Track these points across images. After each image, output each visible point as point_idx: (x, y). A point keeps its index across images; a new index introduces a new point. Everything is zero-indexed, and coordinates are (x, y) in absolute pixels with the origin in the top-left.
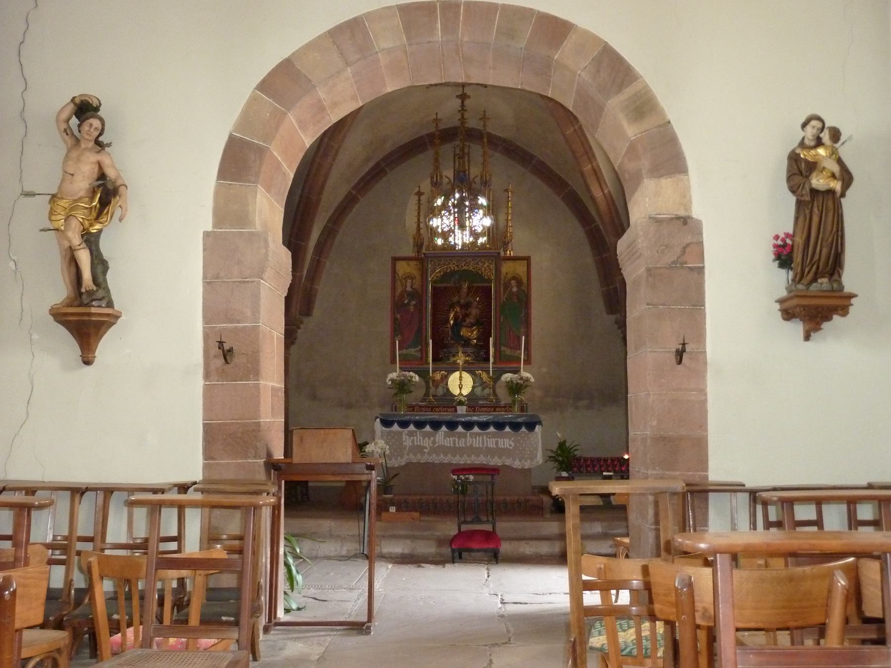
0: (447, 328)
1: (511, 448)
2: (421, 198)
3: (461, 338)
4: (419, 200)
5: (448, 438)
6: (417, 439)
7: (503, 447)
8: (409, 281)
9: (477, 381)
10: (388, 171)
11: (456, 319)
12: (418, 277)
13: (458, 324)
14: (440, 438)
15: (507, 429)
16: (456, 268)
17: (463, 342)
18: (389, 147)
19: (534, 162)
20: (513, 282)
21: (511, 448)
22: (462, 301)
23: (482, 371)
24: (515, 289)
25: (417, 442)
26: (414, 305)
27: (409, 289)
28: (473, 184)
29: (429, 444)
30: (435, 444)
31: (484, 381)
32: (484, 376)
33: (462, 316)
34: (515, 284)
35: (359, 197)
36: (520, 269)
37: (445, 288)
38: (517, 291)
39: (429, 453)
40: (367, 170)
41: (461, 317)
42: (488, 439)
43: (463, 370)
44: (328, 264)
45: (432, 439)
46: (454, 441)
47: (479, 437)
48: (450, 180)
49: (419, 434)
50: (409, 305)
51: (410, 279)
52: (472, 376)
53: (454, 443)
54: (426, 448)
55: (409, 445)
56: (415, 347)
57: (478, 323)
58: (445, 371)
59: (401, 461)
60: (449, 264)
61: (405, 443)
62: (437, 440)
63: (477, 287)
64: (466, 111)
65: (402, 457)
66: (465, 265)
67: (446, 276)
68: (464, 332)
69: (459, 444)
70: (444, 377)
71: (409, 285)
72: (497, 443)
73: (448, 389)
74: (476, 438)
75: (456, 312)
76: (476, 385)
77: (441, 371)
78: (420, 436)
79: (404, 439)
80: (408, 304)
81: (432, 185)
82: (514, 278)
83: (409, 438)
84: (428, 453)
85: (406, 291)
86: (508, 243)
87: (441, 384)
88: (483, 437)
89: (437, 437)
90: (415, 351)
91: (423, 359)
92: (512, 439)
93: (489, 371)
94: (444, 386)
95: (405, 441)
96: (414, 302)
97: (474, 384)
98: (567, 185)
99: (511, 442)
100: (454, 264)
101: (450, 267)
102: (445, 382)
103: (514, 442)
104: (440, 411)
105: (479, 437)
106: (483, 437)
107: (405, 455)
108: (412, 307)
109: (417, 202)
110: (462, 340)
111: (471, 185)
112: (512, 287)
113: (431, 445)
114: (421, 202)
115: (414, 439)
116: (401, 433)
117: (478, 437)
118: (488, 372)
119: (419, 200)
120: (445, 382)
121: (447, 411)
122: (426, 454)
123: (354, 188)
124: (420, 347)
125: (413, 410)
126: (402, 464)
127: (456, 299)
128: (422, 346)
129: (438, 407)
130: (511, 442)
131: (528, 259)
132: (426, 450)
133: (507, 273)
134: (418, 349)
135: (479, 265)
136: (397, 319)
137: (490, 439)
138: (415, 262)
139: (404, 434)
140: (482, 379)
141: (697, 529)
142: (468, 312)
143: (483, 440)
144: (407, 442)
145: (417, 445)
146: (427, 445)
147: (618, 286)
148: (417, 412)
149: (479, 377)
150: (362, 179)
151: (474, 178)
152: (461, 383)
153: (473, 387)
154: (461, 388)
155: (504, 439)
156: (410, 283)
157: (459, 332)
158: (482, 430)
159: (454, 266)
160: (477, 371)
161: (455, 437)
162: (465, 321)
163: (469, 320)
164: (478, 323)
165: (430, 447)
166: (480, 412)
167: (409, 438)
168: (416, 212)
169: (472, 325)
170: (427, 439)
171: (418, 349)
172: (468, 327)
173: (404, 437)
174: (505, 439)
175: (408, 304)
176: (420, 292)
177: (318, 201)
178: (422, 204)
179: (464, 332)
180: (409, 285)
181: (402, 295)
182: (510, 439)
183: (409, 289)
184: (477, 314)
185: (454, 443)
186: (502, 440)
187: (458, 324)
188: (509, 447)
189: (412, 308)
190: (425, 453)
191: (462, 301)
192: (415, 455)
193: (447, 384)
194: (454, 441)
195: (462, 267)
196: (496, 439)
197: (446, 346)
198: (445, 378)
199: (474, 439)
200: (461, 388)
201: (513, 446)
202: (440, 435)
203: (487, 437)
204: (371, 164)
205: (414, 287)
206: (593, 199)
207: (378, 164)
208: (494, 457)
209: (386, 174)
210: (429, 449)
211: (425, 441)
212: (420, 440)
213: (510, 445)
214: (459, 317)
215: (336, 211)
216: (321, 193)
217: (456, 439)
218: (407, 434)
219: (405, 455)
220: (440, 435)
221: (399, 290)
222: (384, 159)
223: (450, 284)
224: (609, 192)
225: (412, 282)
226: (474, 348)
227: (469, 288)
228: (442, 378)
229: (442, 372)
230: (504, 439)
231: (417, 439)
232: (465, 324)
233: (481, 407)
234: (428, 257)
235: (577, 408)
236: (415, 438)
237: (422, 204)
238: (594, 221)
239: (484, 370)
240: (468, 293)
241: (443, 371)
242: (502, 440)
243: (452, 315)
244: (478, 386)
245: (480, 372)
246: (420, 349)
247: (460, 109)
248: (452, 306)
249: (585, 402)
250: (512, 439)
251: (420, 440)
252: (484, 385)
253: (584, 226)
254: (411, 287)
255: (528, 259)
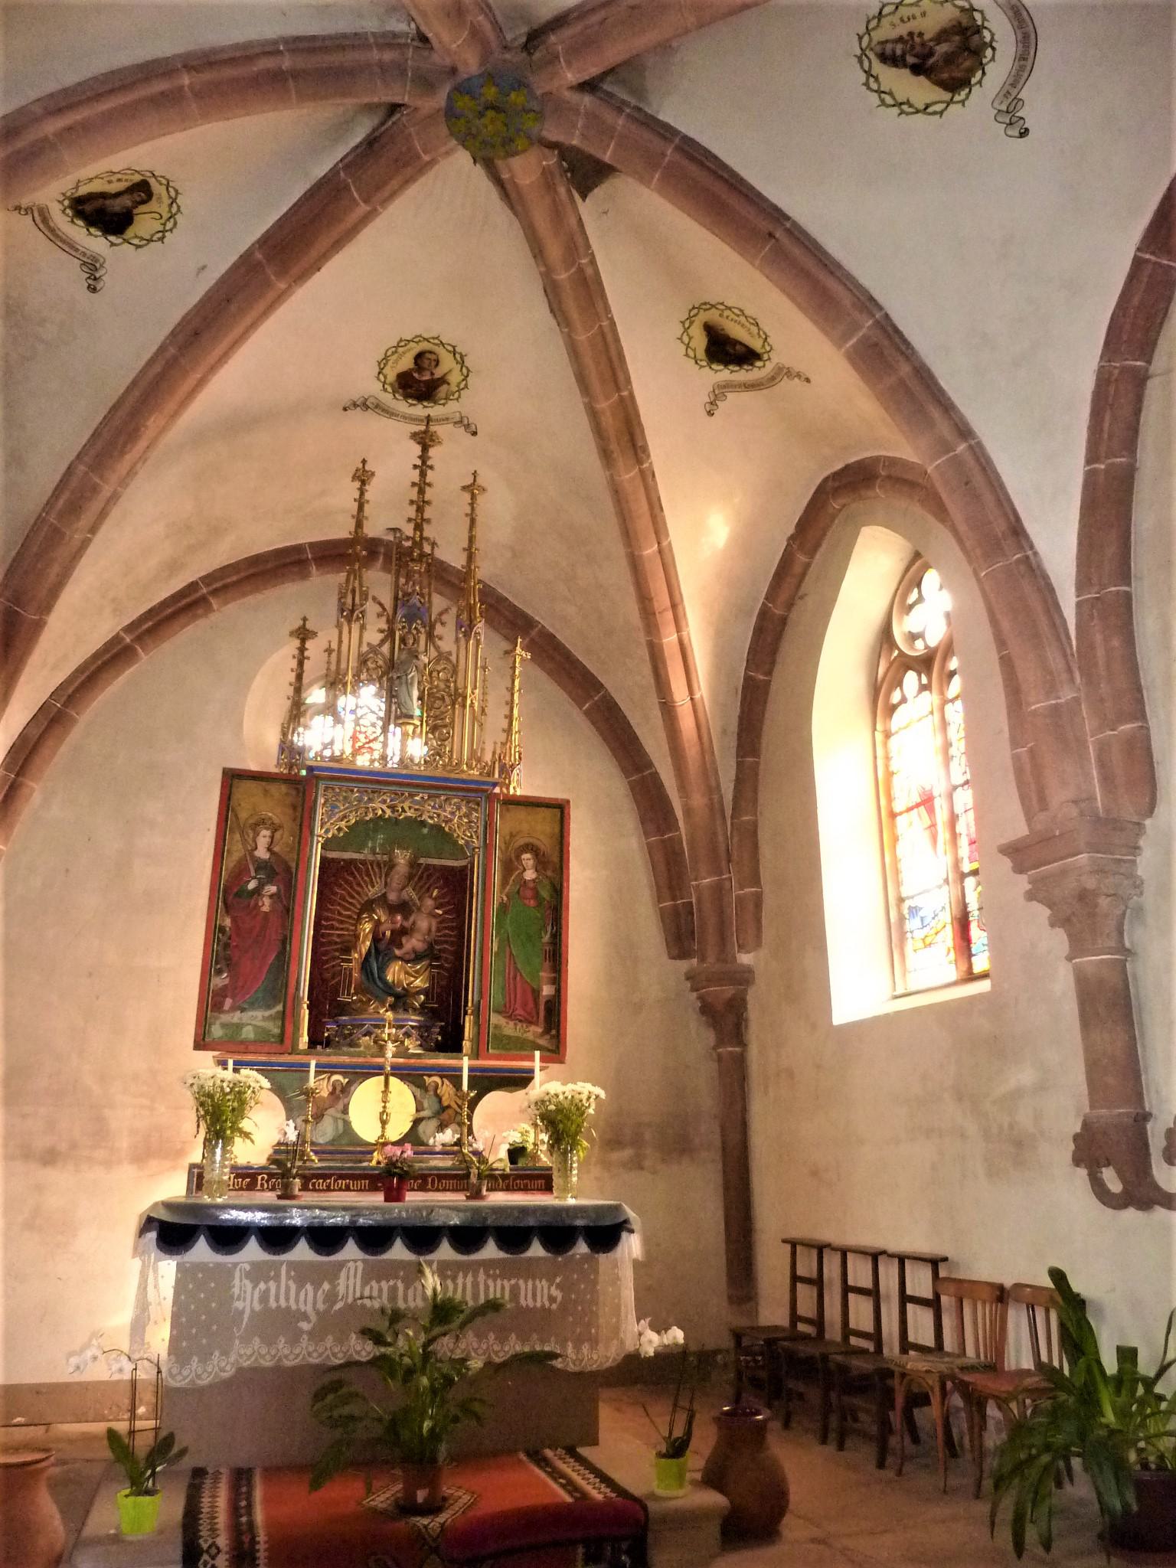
0: (350, 961)
1: (554, 1306)
2: (307, 646)
3: (388, 989)
4: (302, 649)
5: (374, 1283)
6: (278, 1287)
7: (531, 1304)
8: (265, 833)
9: (426, 1105)
10: (215, 606)
11: (376, 940)
12: (288, 824)
13: (383, 950)
14: (351, 1281)
15: (536, 1250)
16: (388, 812)
17: (390, 999)
18: (224, 553)
19: (534, 633)
20: (526, 856)
21: (554, 1306)
22: (392, 897)
23: (441, 1077)
24: (530, 875)
25: (277, 1300)
26: (271, 896)
27: (262, 853)
28: (438, 626)
29: (315, 1303)
30: (335, 1303)
31: (445, 1104)
32: (446, 1090)
33: (393, 932)
34: (531, 862)
35: (140, 650)
36: (540, 828)
37: (351, 862)
38: (534, 881)
39: (316, 1335)
40: (164, 594)
41: (388, 933)
42: (490, 1283)
43: (393, 1075)
44: (37, 798)
45: (326, 1286)
46: (393, 1290)
47: (465, 1277)
48: (384, 609)
49: (288, 1272)
50: (259, 895)
51: (267, 829)
52: (414, 1088)
53: (393, 1297)
54: (305, 1317)
55: (252, 1310)
56: (269, 1007)
57: (428, 955)
58: (344, 1074)
59: (223, 1364)
60: (370, 800)
61: (239, 1305)
62: (341, 1289)
63: (428, 867)
64: (431, 467)
65: (225, 1353)
66: (410, 808)
67: (360, 832)
68: (395, 973)
69: (405, 1300)
70: (339, 1088)
71: (263, 840)
72: (515, 1292)
73: (347, 1124)
74: (460, 1281)
75: (378, 924)
76: (423, 1114)
77: (333, 1073)
78: (289, 1277)
79: (236, 1291)
80: (257, 891)
81: (343, 611)
82: (529, 848)
83: (254, 1288)
84: (311, 1334)
85: (255, 860)
86: (512, 767)
87: (331, 1111)
88: (475, 1277)
89: (342, 1281)
90: (264, 1019)
91: (284, 1040)
92: (558, 1280)
93: (460, 1077)
94: (339, 1115)
95: (238, 1299)
96: (273, 889)
97: (417, 1111)
98: (598, 686)
99: (553, 1288)
100: (384, 801)
101: (374, 810)
102: (340, 1106)
103: (562, 1290)
104: (329, 1189)
105: (465, 1277)
106: (475, 1277)
107: (237, 1342)
108: (267, 901)
109: (296, 652)
110: (391, 995)
111: (432, 627)
112: (525, 870)
113: (321, 1306)
114: (306, 654)
115: (267, 1290)
116: (225, 1275)
117: (461, 1274)
118: (456, 1081)
119: (302, 649)
120: (340, 1106)
121: (348, 1189)
122: (305, 1336)
123: (129, 628)
124: (280, 1008)
125: (251, 1187)
126: (225, 1375)
127: (373, 892)
128: (284, 1007)
129: (325, 1177)
130: (553, 1288)
131: (560, 809)
132: (305, 1326)
133: (512, 835)
134: (273, 1011)
135: (445, 811)
136: (222, 930)
137: (495, 1281)
138: (284, 788)
139: (237, 1274)
140: (439, 1099)
141: (887, 1463)
142: (407, 924)
143: (475, 1285)
144: (246, 1297)
145: (279, 1307)
146: (309, 1309)
147: (694, 900)
148: (263, 1190)
149: (432, 1093)
150: (151, 613)
151: (441, 614)
152: (385, 1107)
153: (417, 1122)
154: (384, 1123)
155: (534, 1280)
156: (268, 839)
157: (382, 969)
158: (462, 1253)
159: (384, 807)
160: (430, 1076)
161: (397, 1277)
162: (400, 946)
163: (414, 943)
164: (428, 955)
165: (318, 1313)
166: (438, 1190)
167: (254, 1288)
168: (294, 674)
169: (417, 957)
170: (309, 1287)
171: (273, 1011)
172: (408, 962)
173: (237, 1282)
174: (538, 1282)
175: (257, 891)
176: (293, 865)
177: (38, 626)
178: (308, 658)
179: (395, 973)
180: (263, 840)
181: (240, 873)
182: (551, 1282)
183: (262, 853)
184: (430, 930)
185: (393, 1297)
186: (530, 1283)
187: (383, 950)
188: (547, 1304)
189: (266, 905)
190: (302, 1332)
191: (392, 897)
192: (270, 1342)
193: (345, 1111)
194: (393, 1290)
195: (404, 810)
196: (513, 1282)
197: (343, 1009)
198: (342, 1094)
199: (449, 1282)
200: (384, 1123)
201: (559, 1299)
202: (352, 1272)
203: (488, 1276)
204: (177, 584)
205: (276, 849)
206: (668, 709)
207: (192, 587)
208: (506, 1338)
209: (209, 609)
210: (313, 1318)
211: (302, 1294)
212: (288, 1289)
213: (552, 1299)
214: (384, 934)
215: (80, 670)
216: (47, 608)
217: (400, 1285)
218: (248, 1275)
219: (237, 1342)
220: (352, 1272)
221: (236, 851)
222: (208, 579)
223: (365, 855)
224: (702, 697)
225: (272, 837)
226: (420, 1014)
227: (413, 864)
228: (332, 1093)
229: (336, 1077)
230: (534, 1280)
231: (278, 1287)
232: (397, 952)
233: (440, 1177)
234: (318, 778)
235: (606, 1165)
236: (272, 1285)
237: (308, 658)
238: (650, 765)
239: (446, 1077)
240: (410, 877)
241: (336, 1073)
242: (530, 1283)
243: (368, 927)
244: (429, 1118)
245: (437, 1079)
246: (278, 1012)
247: (419, 462)
248: (368, 907)
249: (627, 1153)
250: (558, 1280)
251: (288, 1289)
252: (445, 1116)
253: (626, 772)
254: (269, 849)
255: (560, 809)
